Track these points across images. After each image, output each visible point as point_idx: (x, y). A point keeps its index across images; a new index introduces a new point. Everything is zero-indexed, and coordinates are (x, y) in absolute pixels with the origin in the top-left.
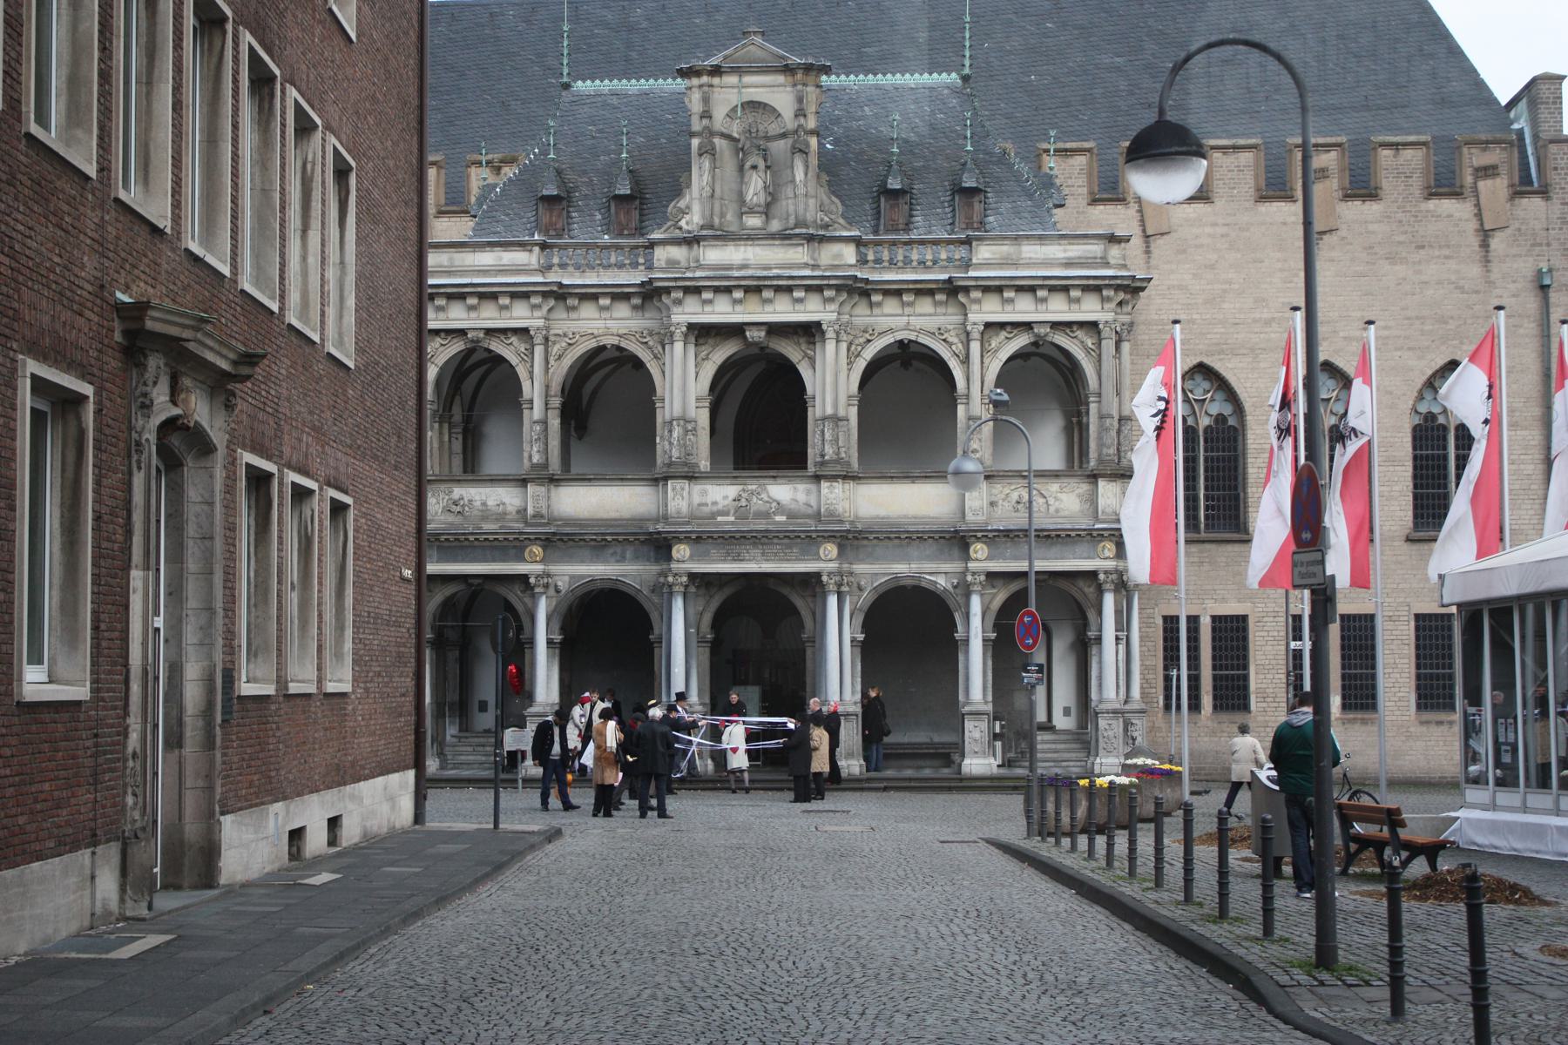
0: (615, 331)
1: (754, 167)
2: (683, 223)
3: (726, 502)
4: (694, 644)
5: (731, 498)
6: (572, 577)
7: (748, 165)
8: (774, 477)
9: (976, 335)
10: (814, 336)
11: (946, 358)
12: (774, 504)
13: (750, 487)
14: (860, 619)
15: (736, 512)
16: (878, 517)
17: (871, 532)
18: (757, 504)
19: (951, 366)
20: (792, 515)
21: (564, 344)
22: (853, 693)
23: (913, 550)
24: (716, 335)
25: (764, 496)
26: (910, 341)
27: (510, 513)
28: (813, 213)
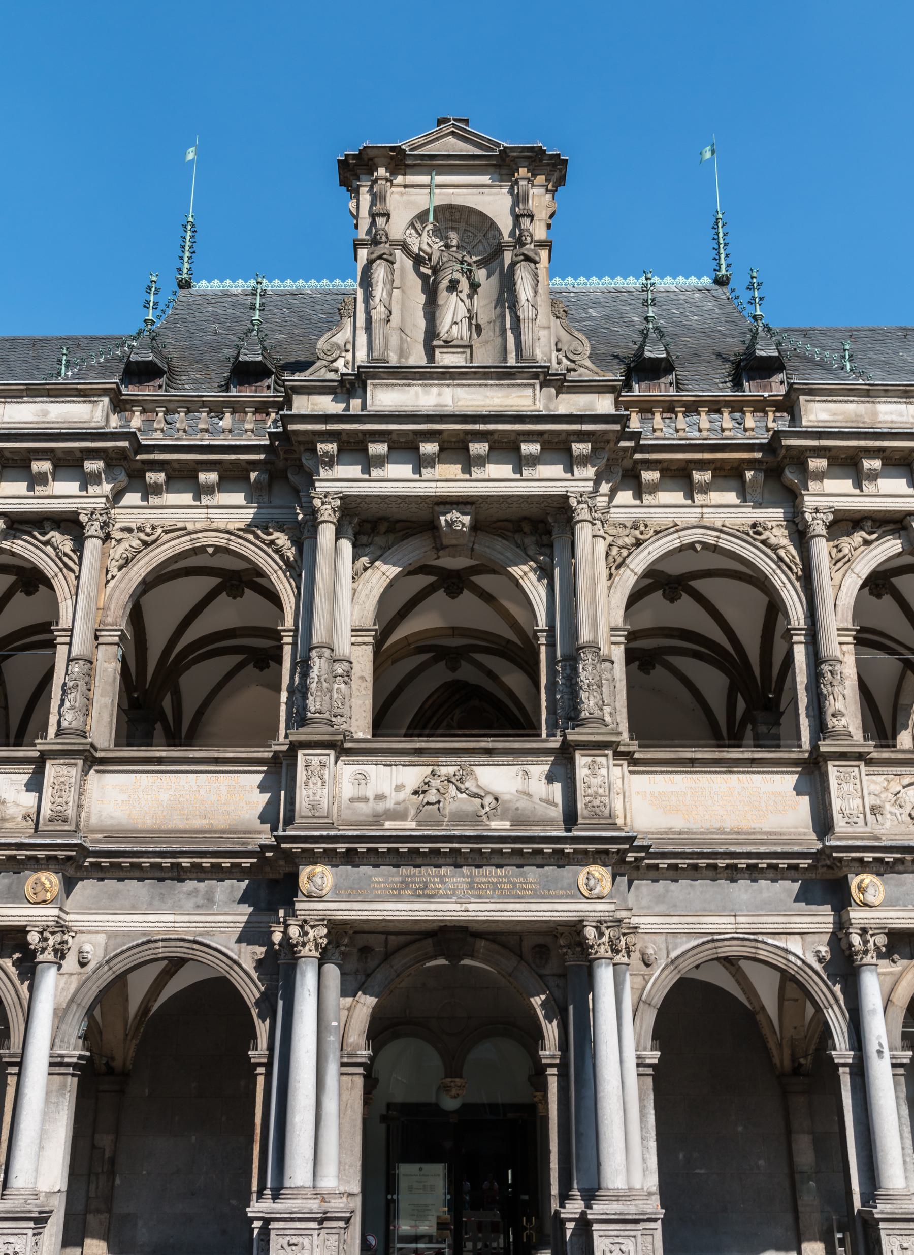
0: (222, 526)
1: (453, 286)
2: (340, 364)
3: (402, 796)
4: (332, 1069)
5: (409, 790)
6: (111, 935)
7: (445, 283)
8: (489, 752)
9: (819, 528)
10: (549, 533)
11: (768, 571)
12: (488, 800)
13: (444, 770)
14: (649, 1017)
15: (419, 811)
16: (669, 831)
17: (663, 855)
18: (455, 801)
19: (778, 584)
20: (517, 822)
21: (136, 543)
22: (645, 1170)
23: (743, 890)
24: (388, 531)
25: (469, 784)
26: (705, 545)
27: (13, 818)
28: (547, 349)
